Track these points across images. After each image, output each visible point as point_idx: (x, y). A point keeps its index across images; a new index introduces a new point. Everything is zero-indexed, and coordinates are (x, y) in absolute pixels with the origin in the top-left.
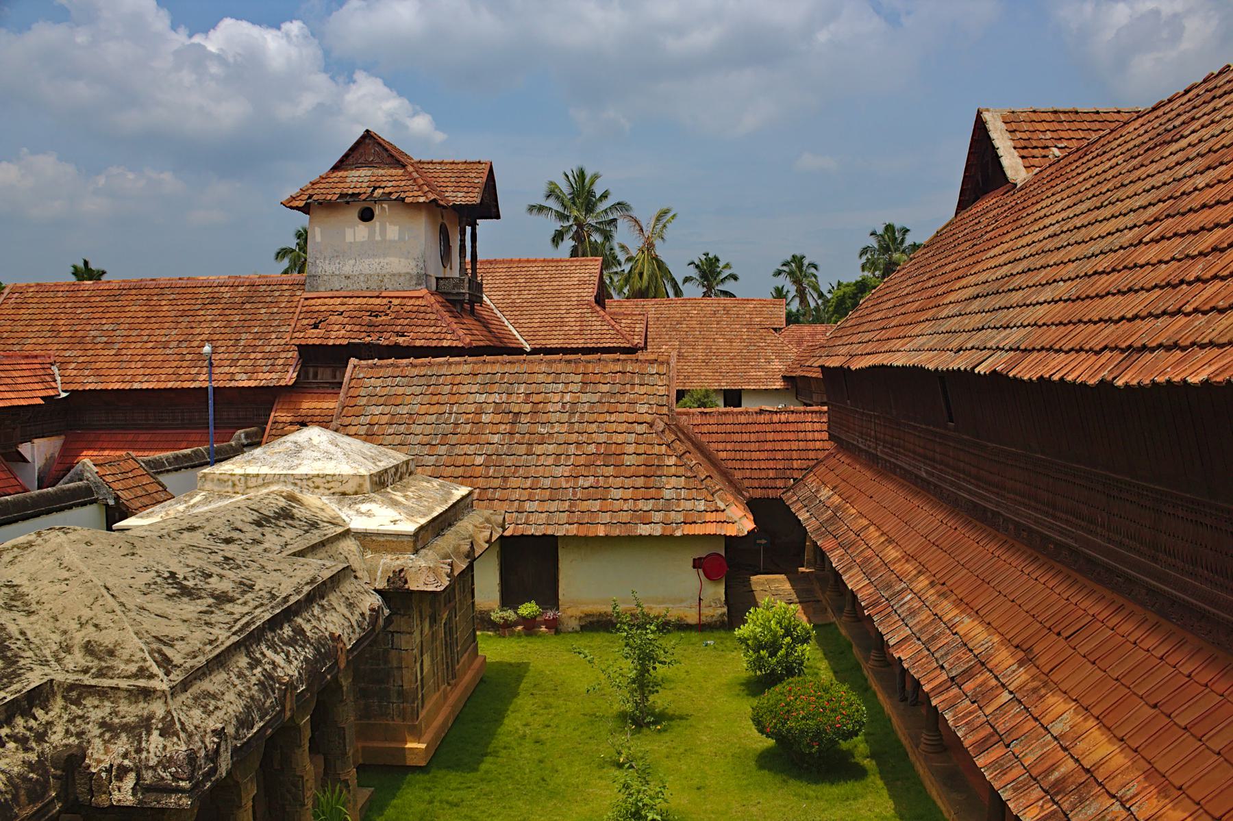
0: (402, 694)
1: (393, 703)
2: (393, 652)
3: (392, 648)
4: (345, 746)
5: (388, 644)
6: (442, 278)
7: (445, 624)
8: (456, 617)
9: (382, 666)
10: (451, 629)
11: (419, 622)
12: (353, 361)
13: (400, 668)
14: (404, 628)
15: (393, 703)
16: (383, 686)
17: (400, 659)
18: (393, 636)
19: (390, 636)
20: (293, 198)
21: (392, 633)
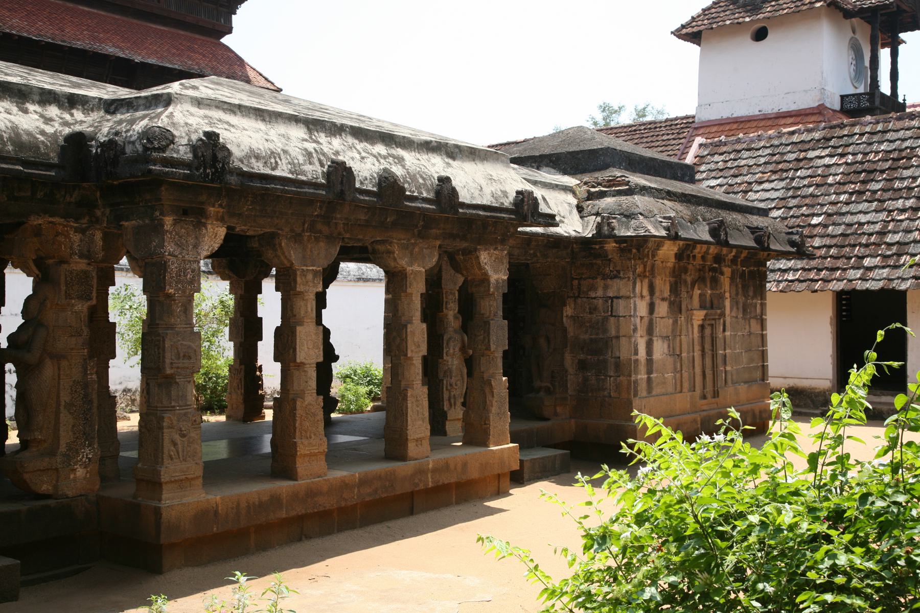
0: (618, 365)
1: (610, 377)
2: (612, 319)
3: (612, 315)
4: (489, 341)
5: (608, 312)
6: (847, 96)
7: (702, 327)
8: (724, 330)
9: (601, 336)
10: (713, 339)
11: (645, 292)
12: (699, 140)
13: (618, 337)
14: (623, 292)
15: (610, 377)
16: (601, 358)
17: (618, 329)
18: (612, 302)
19: (610, 301)
20: (683, 27)
21: (612, 298)
